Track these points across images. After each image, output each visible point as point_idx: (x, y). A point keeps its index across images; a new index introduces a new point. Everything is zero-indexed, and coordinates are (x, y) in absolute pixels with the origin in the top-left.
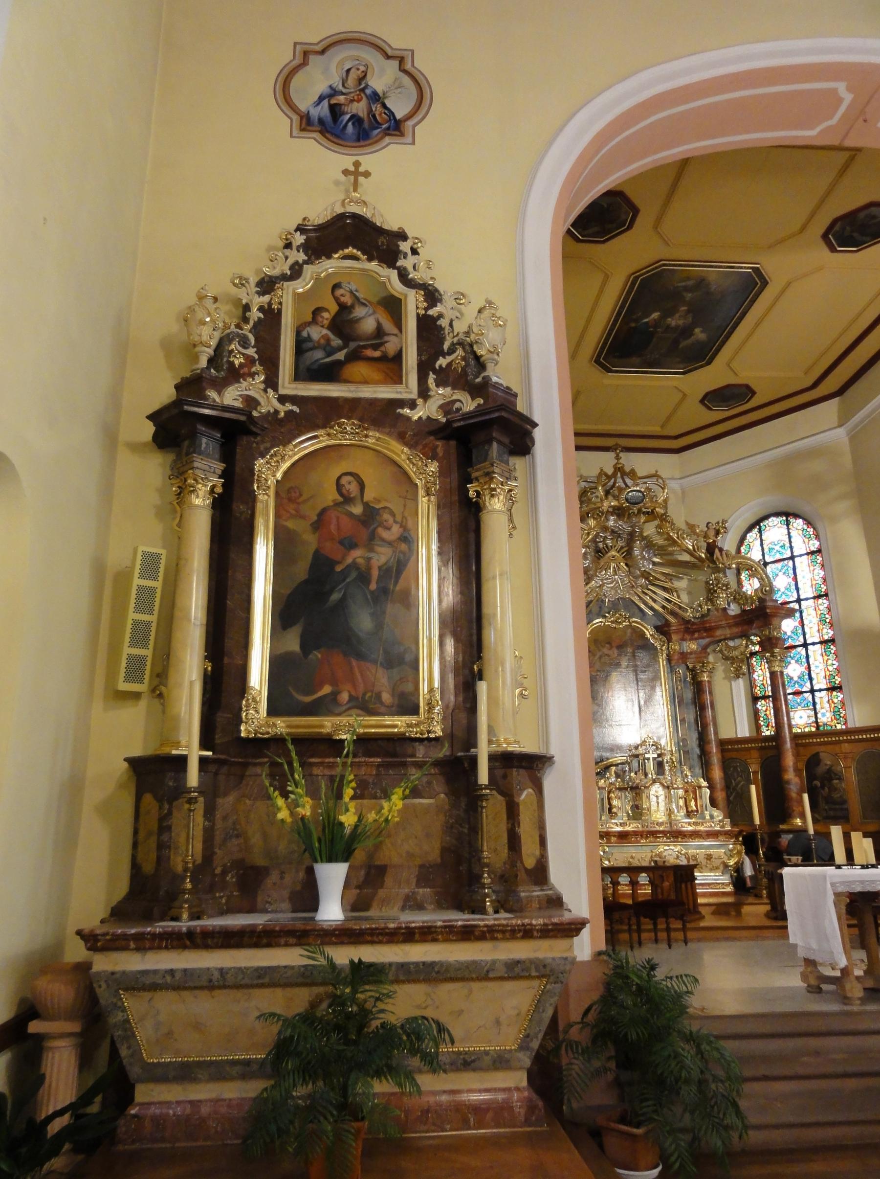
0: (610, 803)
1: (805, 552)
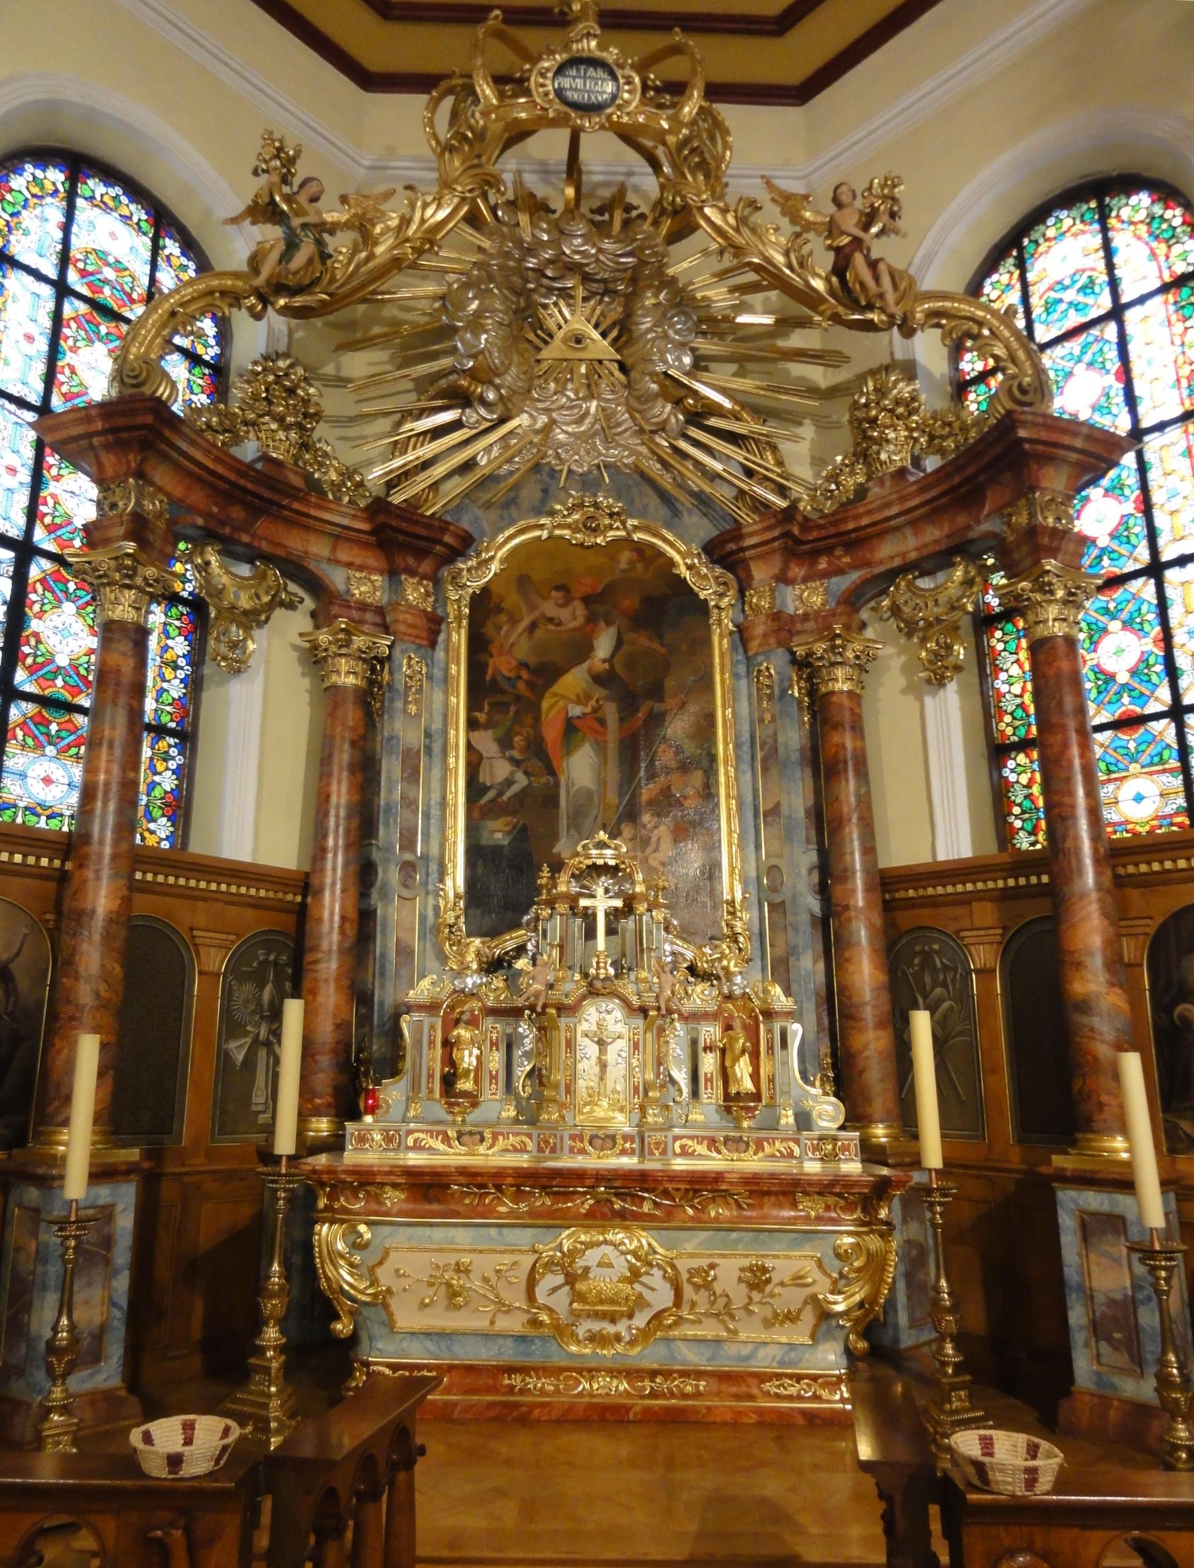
0: (449, 1061)
1: (1157, 284)
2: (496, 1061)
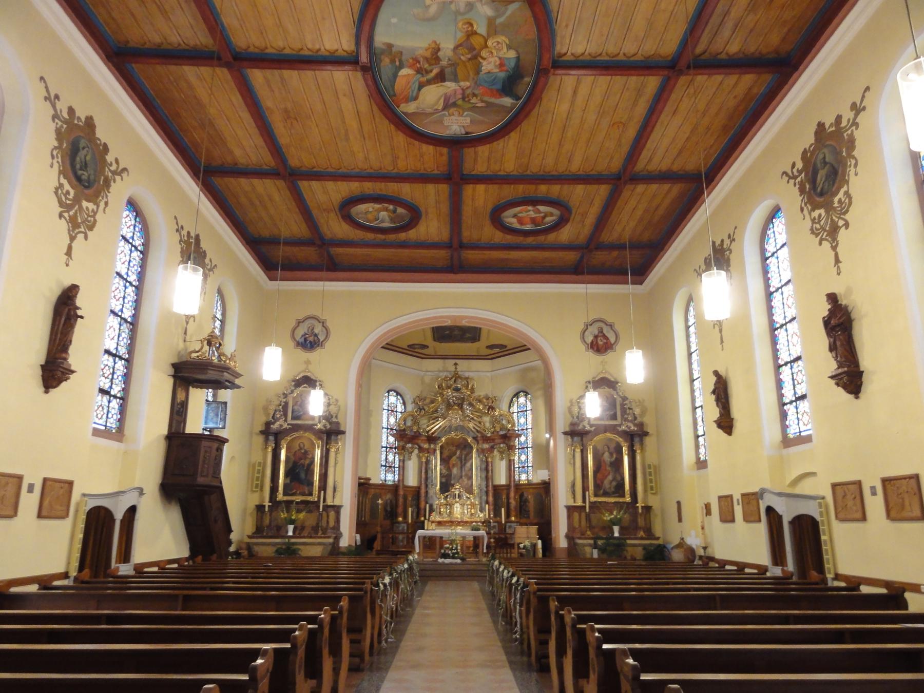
0: (440, 510)
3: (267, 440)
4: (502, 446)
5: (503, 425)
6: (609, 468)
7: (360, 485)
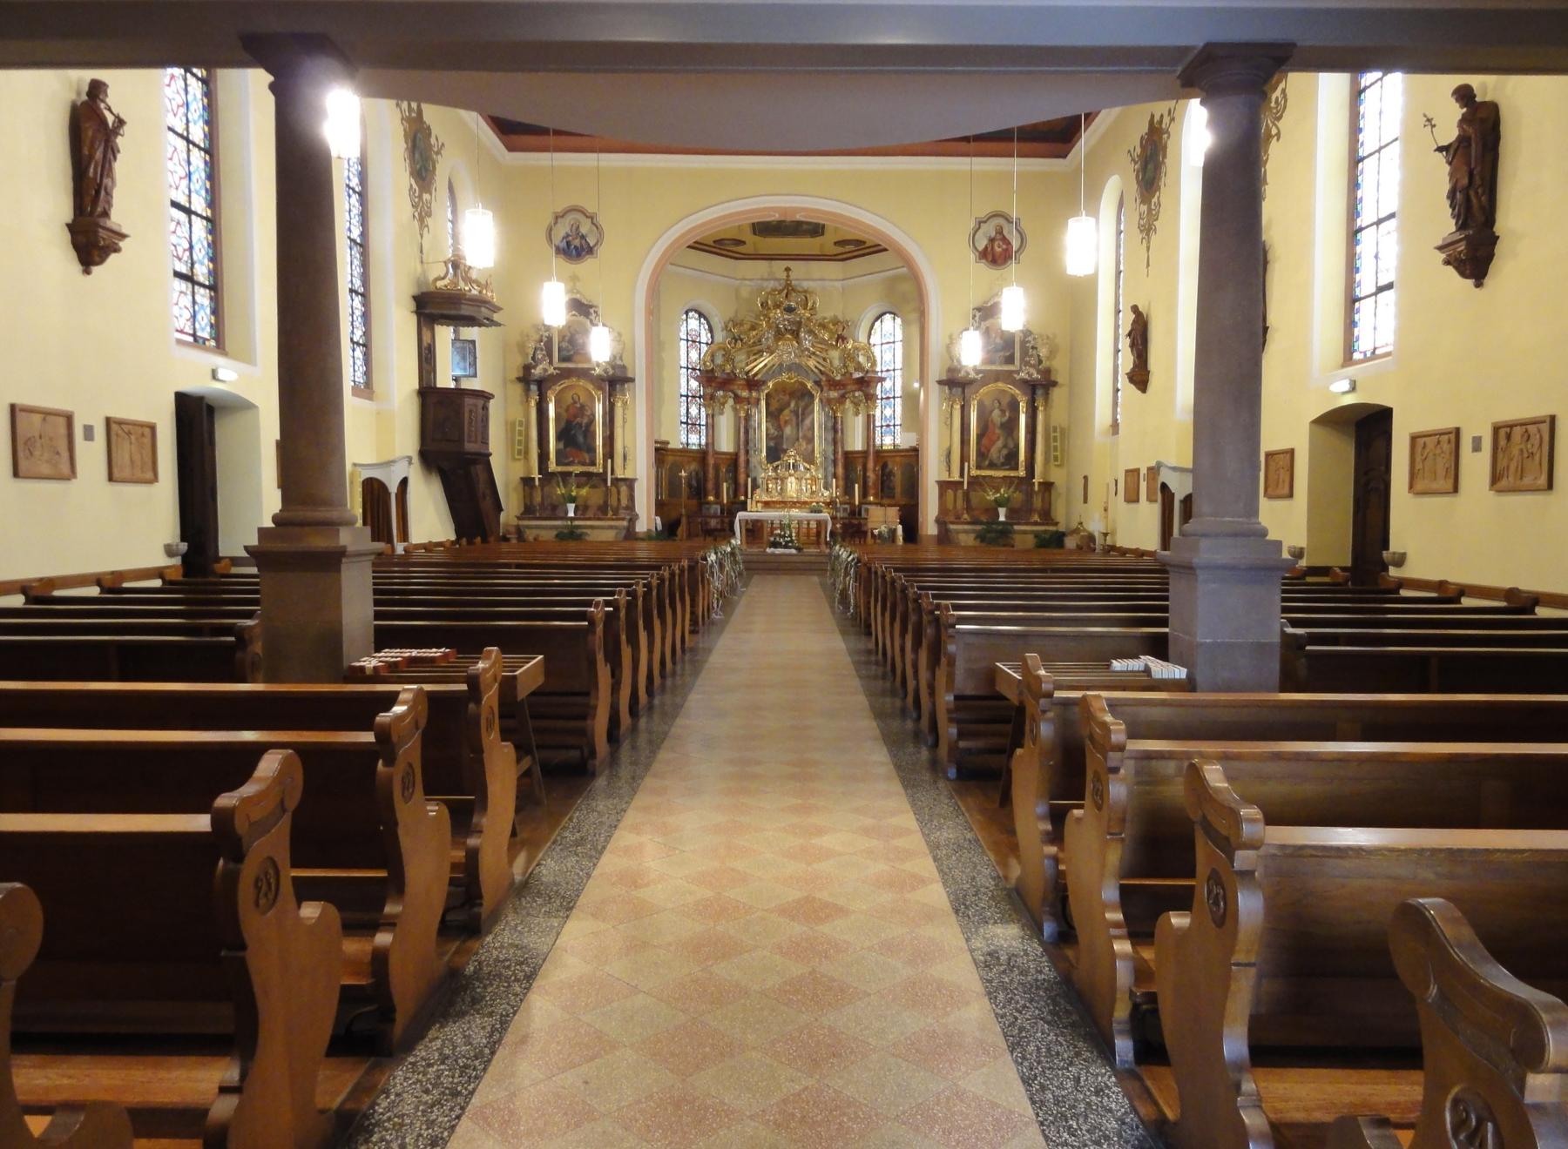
0: (768, 487)
2: (774, 486)
3: (527, 391)
4: (857, 394)
5: (859, 362)
6: (998, 431)
7: (657, 450)
